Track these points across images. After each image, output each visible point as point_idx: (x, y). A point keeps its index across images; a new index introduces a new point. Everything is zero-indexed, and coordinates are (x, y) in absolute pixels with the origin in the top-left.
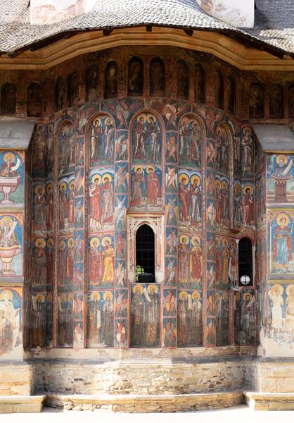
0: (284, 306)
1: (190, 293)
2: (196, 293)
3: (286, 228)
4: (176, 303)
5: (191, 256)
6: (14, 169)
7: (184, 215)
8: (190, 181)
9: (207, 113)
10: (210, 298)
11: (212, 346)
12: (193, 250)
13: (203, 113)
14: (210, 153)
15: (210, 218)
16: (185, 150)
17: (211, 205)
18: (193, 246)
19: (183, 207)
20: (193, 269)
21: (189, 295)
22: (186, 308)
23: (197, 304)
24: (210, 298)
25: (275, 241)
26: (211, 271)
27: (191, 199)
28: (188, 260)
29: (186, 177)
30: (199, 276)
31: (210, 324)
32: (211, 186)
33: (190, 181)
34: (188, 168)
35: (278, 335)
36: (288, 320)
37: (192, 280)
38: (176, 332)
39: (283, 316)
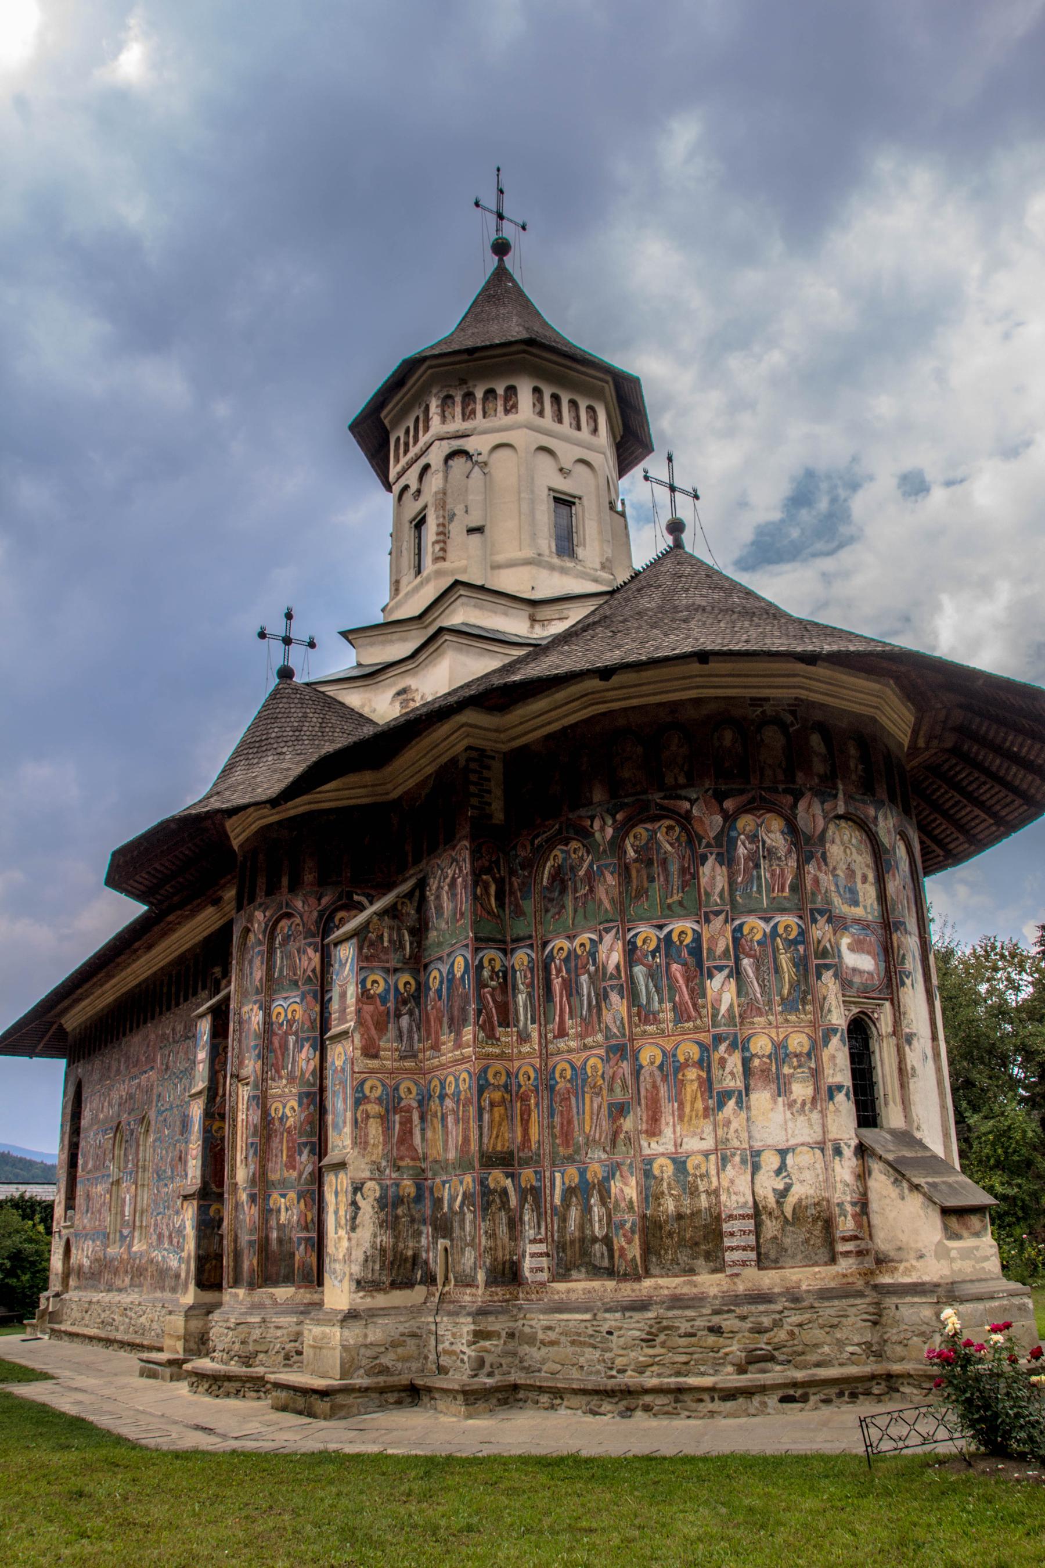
0: (336, 1212)
1: (284, 1196)
2: (292, 1195)
3: (343, 1070)
4: (257, 1215)
5: (285, 1134)
6: (205, 1038)
7: (278, 1072)
8: (286, 1016)
9: (304, 903)
10: (302, 1201)
11: (306, 1287)
12: (288, 1124)
13: (299, 904)
14: (306, 963)
15: (304, 1067)
16: (281, 971)
17: (307, 1045)
18: (288, 1118)
19: (277, 1058)
20: (288, 1156)
21: (283, 1200)
22: (278, 1220)
23: (292, 1215)
24: (302, 1201)
25: (334, 1096)
26: (304, 1157)
27: (286, 1042)
28: (281, 1142)
29: (280, 1010)
30: (294, 1168)
31: (302, 1247)
32: (306, 1016)
33: (286, 1016)
34: (285, 995)
35: (333, 1266)
36: (339, 1238)
37: (286, 1174)
38: (255, 1262)
39: (336, 1233)
